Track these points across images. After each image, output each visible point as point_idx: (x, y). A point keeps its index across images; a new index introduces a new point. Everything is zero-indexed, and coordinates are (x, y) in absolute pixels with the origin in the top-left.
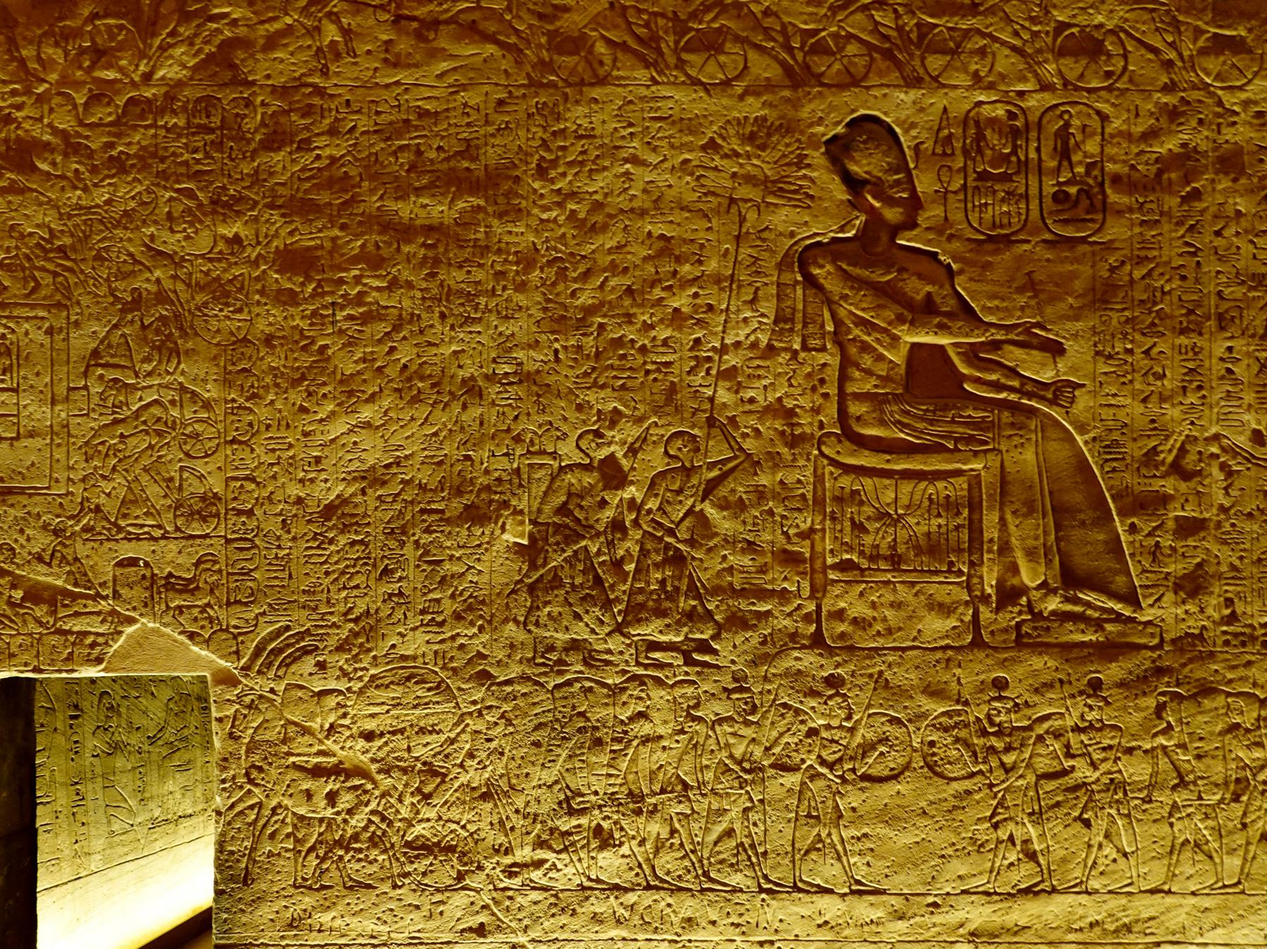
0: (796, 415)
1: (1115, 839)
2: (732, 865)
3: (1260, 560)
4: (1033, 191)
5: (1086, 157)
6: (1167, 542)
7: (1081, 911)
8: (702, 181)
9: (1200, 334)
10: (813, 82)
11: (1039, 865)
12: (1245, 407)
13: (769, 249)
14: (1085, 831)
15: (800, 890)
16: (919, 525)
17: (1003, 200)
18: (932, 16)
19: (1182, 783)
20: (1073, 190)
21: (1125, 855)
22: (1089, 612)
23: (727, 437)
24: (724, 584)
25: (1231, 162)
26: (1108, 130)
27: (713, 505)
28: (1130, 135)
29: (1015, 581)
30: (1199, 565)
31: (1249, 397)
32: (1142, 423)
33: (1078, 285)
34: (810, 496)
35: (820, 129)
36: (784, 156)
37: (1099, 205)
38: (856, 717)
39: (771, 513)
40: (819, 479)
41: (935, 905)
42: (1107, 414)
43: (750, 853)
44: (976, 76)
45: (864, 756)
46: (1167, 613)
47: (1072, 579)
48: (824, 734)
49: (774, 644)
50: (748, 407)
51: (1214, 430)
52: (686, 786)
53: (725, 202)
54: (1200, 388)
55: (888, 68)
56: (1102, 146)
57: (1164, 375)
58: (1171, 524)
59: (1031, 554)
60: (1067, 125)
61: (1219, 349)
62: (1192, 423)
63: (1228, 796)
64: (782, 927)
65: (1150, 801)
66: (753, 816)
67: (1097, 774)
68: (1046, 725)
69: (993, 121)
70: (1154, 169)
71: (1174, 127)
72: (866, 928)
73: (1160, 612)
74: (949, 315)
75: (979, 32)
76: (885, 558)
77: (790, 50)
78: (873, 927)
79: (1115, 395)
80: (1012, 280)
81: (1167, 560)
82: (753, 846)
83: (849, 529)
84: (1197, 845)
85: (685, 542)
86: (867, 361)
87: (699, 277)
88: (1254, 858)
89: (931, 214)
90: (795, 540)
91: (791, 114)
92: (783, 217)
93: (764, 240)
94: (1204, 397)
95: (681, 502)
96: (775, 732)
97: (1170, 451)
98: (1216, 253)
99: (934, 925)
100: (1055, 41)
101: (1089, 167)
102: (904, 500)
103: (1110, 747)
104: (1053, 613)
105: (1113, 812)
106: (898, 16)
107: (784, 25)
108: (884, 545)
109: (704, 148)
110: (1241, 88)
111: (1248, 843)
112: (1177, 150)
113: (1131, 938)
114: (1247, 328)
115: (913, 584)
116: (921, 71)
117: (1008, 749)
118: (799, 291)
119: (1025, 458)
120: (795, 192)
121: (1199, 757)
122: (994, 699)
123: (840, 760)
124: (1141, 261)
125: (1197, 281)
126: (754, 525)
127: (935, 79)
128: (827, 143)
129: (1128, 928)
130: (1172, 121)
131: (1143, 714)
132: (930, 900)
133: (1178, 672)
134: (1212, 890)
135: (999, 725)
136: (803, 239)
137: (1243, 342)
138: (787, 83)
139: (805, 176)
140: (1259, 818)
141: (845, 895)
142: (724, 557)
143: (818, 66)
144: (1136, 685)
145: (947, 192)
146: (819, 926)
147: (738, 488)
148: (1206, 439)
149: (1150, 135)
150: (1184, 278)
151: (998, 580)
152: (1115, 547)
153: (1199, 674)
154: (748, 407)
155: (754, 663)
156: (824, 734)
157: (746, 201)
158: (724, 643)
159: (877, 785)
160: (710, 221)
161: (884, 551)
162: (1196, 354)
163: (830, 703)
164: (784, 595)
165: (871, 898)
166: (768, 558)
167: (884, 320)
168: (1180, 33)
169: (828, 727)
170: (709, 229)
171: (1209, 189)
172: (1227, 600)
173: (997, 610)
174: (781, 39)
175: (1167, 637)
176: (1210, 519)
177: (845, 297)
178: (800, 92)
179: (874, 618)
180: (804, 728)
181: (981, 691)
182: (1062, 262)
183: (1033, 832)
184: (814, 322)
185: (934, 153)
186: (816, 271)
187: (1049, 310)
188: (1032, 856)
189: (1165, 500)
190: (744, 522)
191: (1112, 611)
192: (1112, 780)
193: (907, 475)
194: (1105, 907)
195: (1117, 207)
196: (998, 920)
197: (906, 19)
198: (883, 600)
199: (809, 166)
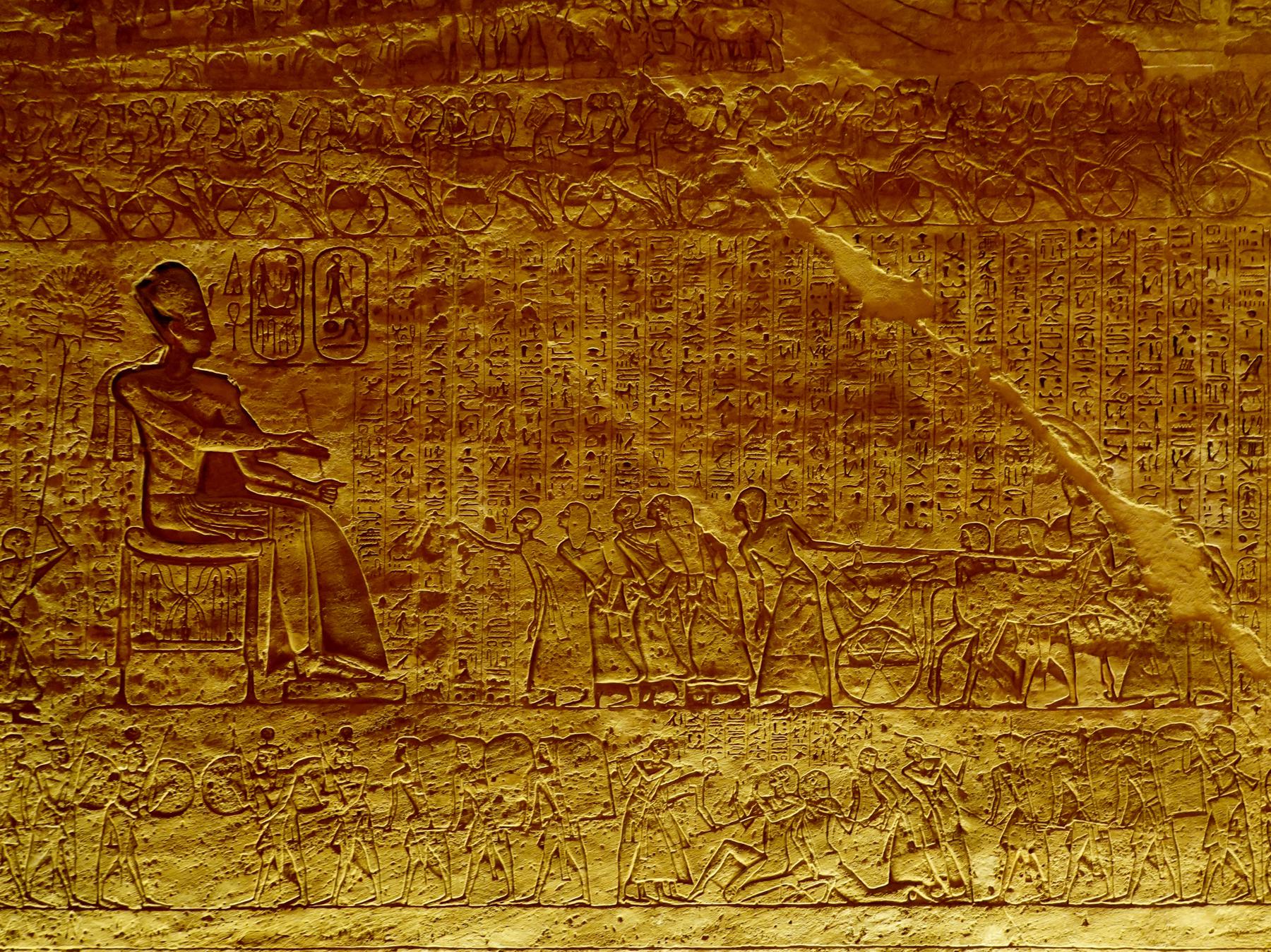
0: (109, 514)
1: (362, 862)
2: (48, 887)
3: (489, 627)
4: (308, 322)
5: (352, 293)
6: (411, 614)
7: (331, 922)
8: (35, 321)
9: (443, 439)
10: (125, 237)
11: (298, 884)
12: (479, 499)
13: (89, 378)
14: (334, 856)
15: (101, 908)
16: (205, 604)
17: (281, 331)
18: (224, 179)
19: (417, 815)
20: (341, 321)
21: (370, 875)
22: (344, 674)
23: (53, 533)
24: (47, 655)
25: (472, 295)
26: (371, 270)
27: (40, 590)
28: (389, 273)
29: (284, 649)
30: (439, 633)
31: (483, 491)
32: (394, 514)
33: (342, 401)
34: (118, 581)
35: (129, 276)
36: (100, 299)
37: (362, 334)
38: (149, 764)
39: (85, 595)
40: (126, 567)
41: (209, 918)
42: (364, 507)
43: (63, 878)
44: (261, 228)
45: (155, 797)
46: (409, 673)
47: (331, 646)
48: (124, 778)
49: (84, 704)
50: (70, 508)
51: (453, 520)
52: (14, 823)
53: (53, 338)
54: (442, 484)
55: (186, 224)
56: (367, 284)
57: (412, 474)
58: (415, 599)
59: (297, 627)
60: (338, 266)
61: (459, 451)
62: (435, 514)
63: (455, 825)
64: (87, 938)
65: (390, 830)
66: (67, 847)
67: (347, 808)
68: (305, 768)
69: (275, 265)
70: (408, 302)
71: (425, 266)
72: (154, 939)
73: (404, 673)
74: (235, 428)
75: (263, 191)
76: (177, 632)
77: (107, 210)
78: (160, 938)
79: (370, 492)
80: (287, 397)
81: (410, 629)
82: (65, 871)
83: (147, 608)
84: (429, 866)
85: (17, 620)
86: (165, 468)
87: (31, 401)
88: (477, 877)
89: (222, 344)
90: (105, 617)
91: (105, 262)
92: (99, 350)
93: (83, 369)
94: (445, 492)
95: (13, 588)
96: (82, 778)
97: (417, 538)
98: (459, 371)
99: (208, 936)
100: (327, 197)
101: (356, 302)
102: (194, 583)
103: (358, 786)
104: (315, 674)
105: (359, 839)
106: (197, 181)
107: (103, 190)
108: (176, 621)
109: (35, 294)
110: (480, 233)
111: (472, 864)
112: (429, 285)
113: (373, 944)
114: (483, 434)
115: (198, 653)
116: (215, 225)
117: (273, 788)
118: (112, 412)
119: (297, 545)
120: (109, 328)
121: (431, 793)
122: (262, 747)
123: (136, 800)
124: (395, 379)
125: (442, 395)
126: (73, 605)
127: (226, 231)
128: (139, 287)
129: (371, 936)
130: (423, 262)
131: (385, 758)
132: (205, 914)
133: (414, 725)
134: (442, 904)
135: (267, 768)
136: (116, 367)
137: (479, 445)
138: (104, 238)
139: (116, 316)
140: (481, 843)
141: (138, 911)
142: (48, 633)
143: (130, 223)
144: (380, 734)
145: (236, 325)
146: (116, 937)
147: (59, 575)
148: (447, 527)
149: (406, 273)
150: (431, 393)
151: (270, 648)
152: (368, 620)
153: (434, 724)
154: (70, 508)
155: (67, 720)
156: (124, 778)
157: (69, 337)
158: (44, 704)
159: (165, 820)
160: (40, 354)
161: (176, 626)
162: (438, 456)
163: (129, 752)
164: (93, 664)
165: (158, 913)
166: (83, 634)
167: (180, 433)
168: (430, 187)
169: (127, 772)
170: (40, 361)
171: (454, 318)
172: (461, 661)
173: (269, 672)
174: (99, 202)
175: (410, 693)
176: (449, 594)
177: (149, 415)
178: (114, 246)
179: (167, 682)
180: (108, 774)
181: (251, 741)
182: (328, 382)
183: (293, 857)
184: (123, 436)
185: (225, 293)
186: (126, 394)
187: (316, 423)
188: (292, 877)
189: (411, 578)
190: (64, 604)
191: (363, 672)
192: (359, 813)
193: (196, 562)
194: (353, 918)
195: (377, 335)
196: (262, 930)
197: (203, 181)
198: (174, 666)
199: (120, 306)
